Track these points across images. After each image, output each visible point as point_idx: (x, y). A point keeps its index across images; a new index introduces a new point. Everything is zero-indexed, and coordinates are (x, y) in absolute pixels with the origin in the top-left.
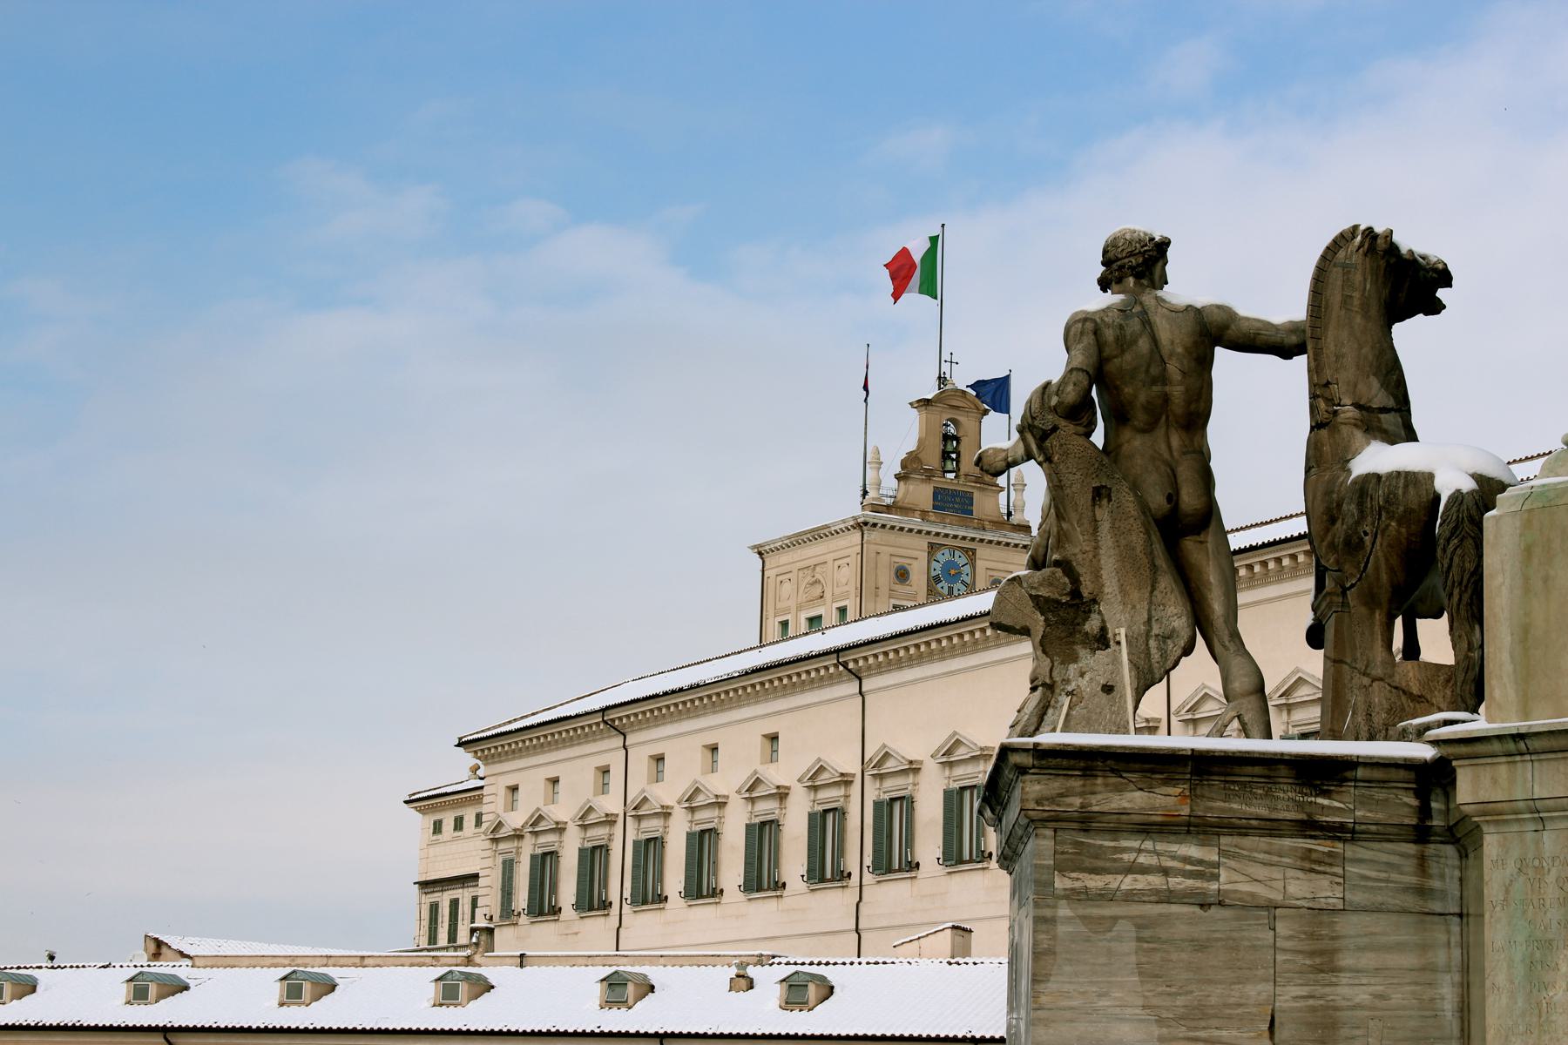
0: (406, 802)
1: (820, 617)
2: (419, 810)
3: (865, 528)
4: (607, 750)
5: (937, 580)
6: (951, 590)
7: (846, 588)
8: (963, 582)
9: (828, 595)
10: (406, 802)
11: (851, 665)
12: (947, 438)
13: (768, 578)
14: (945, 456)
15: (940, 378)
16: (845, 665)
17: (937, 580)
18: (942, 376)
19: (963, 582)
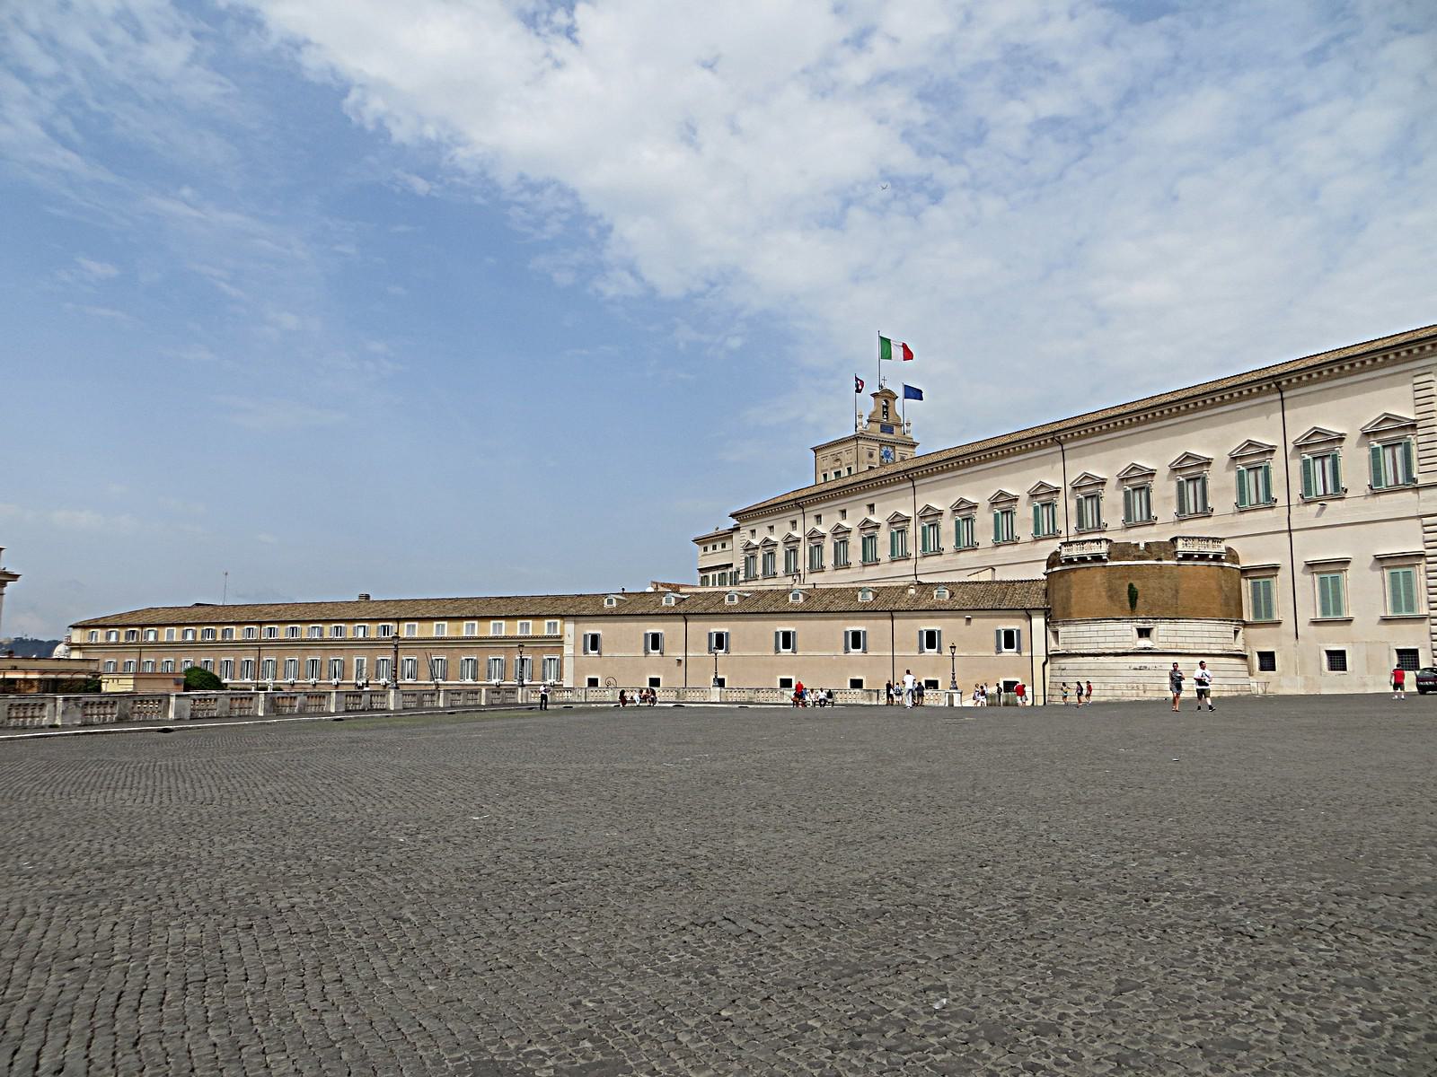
4: (796, 515)
5: (883, 457)
7: (850, 461)
9: (843, 464)
11: (910, 476)
12: (884, 407)
14: (884, 413)
16: (908, 476)
17: (883, 457)
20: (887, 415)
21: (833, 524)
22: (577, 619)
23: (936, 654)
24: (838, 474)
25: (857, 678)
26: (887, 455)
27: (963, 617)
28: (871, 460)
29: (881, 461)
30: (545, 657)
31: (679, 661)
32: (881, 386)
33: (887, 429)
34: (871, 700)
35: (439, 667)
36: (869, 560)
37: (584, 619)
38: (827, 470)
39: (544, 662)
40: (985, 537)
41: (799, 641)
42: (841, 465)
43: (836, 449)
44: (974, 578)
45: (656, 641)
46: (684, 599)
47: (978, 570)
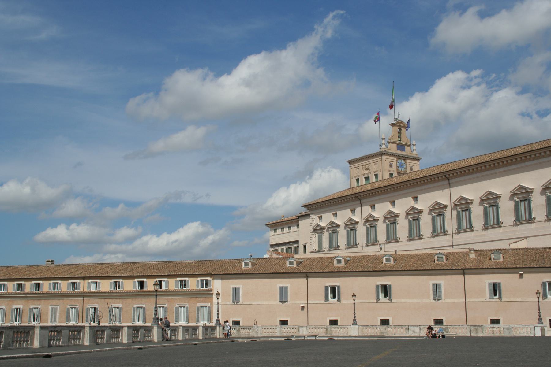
0: (266, 225)
1: (369, 177)
2: (269, 227)
3: (382, 154)
5: (398, 167)
6: (401, 169)
7: (377, 170)
8: (404, 168)
9: (371, 172)
10: (266, 225)
11: (447, 176)
13: (352, 168)
14: (399, 136)
15: (395, 118)
16: (445, 176)
18: (395, 118)
19: (404, 168)
20: (401, 138)
21: (407, 207)
22: (224, 276)
23: (498, 300)
24: (367, 179)
25: (439, 318)
26: (402, 165)
27: (518, 273)
28: (391, 169)
29: (397, 170)
30: (199, 305)
31: (303, 308)
32: (396, 119)
33: (401, 147)
34: (477, 333)
35: (117, 312)
36: (392, 238)
37: (228, 276)
38: (359, 176)
39: (198, 308)
40: (478, 222)
41: (394, 291)
42: (370, 173)
43: (365, 162)
44: (513, 246)
45: (334, 291)
46: (301, 262)
47: (519, 239)
